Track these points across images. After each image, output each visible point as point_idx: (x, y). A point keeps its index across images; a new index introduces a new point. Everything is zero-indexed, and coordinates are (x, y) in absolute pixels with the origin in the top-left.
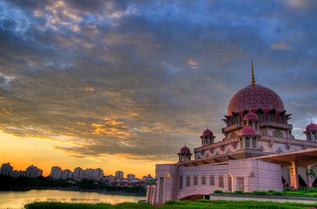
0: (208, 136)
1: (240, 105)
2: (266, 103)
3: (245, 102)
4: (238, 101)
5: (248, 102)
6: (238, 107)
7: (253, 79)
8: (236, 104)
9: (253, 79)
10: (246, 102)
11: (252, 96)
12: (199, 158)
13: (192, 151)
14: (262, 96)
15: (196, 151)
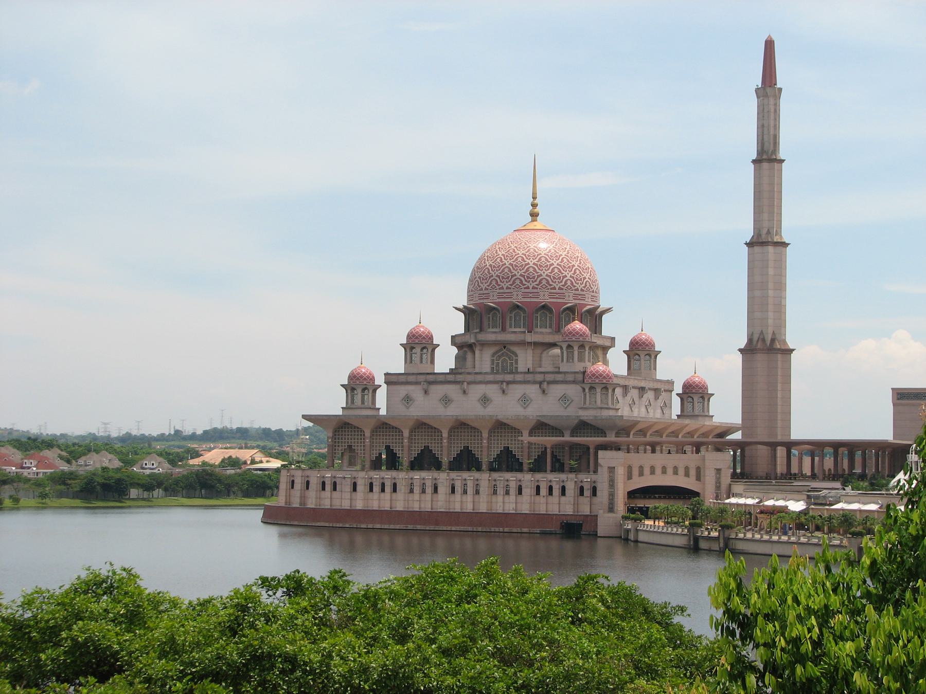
0: (419, 344)
1: (528, 288)
2: (582, 290)
3: (540, 282)
4: (523, 276)
5: (548, 282)
6: (523, 290)
7: (534, 205)
8: (518, 282)
9: (534, 205)
10: (544, 282)
11: (556, 270)
12: (408, 399)
13: (380, 380)
14: (575, 272)
15: (391, 380)
